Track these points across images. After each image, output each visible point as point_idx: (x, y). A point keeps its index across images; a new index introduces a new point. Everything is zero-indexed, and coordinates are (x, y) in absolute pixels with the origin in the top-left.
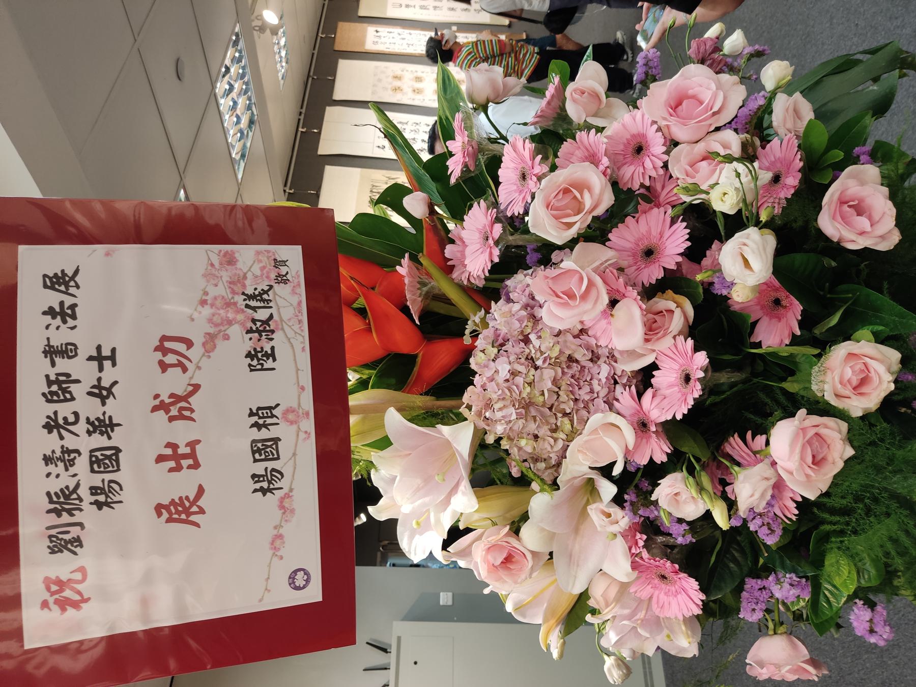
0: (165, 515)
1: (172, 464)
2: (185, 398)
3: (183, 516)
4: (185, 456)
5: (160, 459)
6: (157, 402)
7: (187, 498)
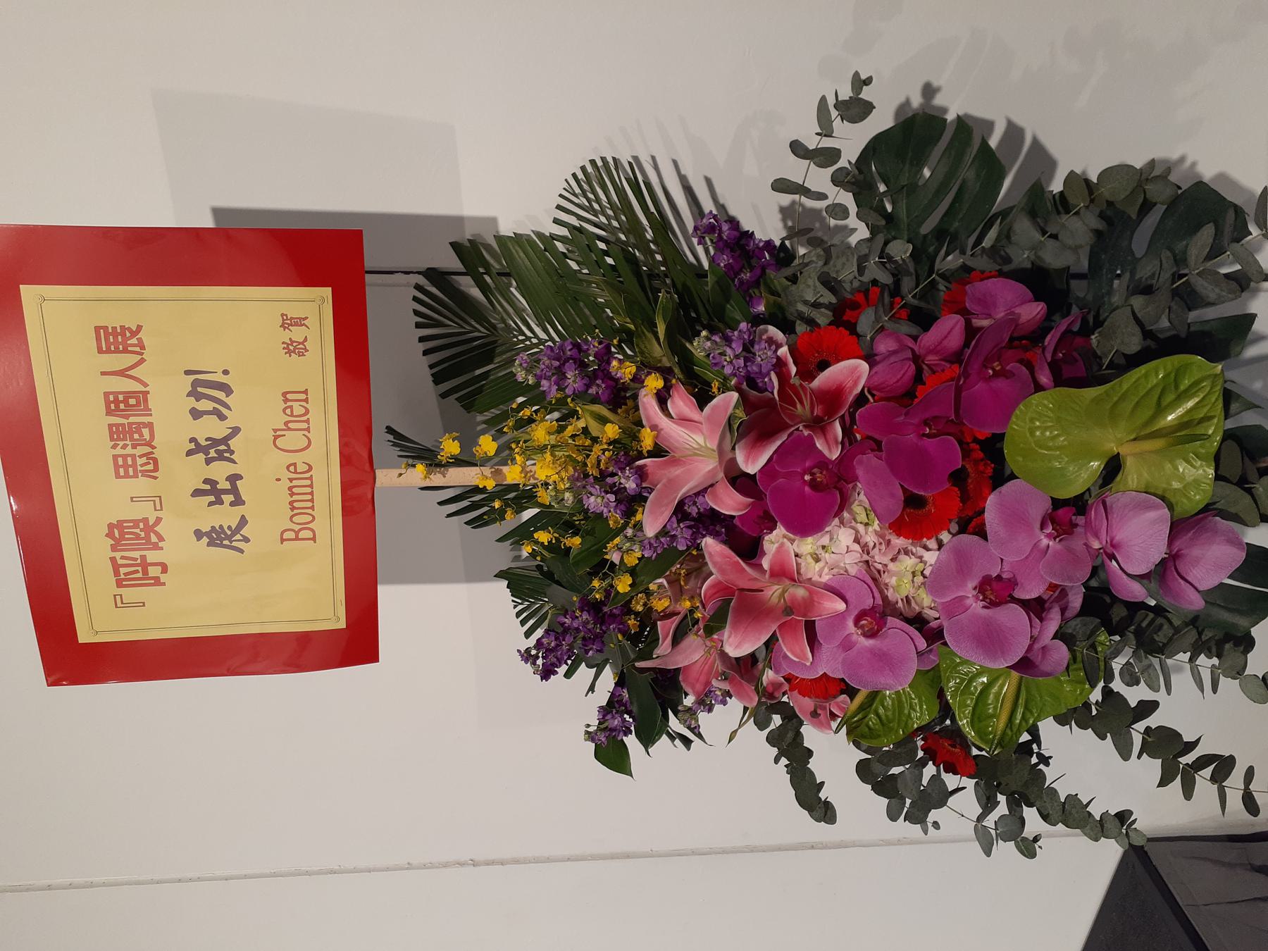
0: (205, 540)
1: (212, 498)
2: (225, 440)
3: (226, 542)
4: (226, 492)
5: (197, 493)
6: (192, 446)
7: (229, 528)
